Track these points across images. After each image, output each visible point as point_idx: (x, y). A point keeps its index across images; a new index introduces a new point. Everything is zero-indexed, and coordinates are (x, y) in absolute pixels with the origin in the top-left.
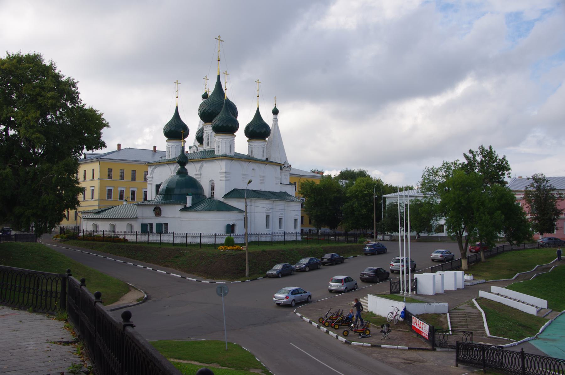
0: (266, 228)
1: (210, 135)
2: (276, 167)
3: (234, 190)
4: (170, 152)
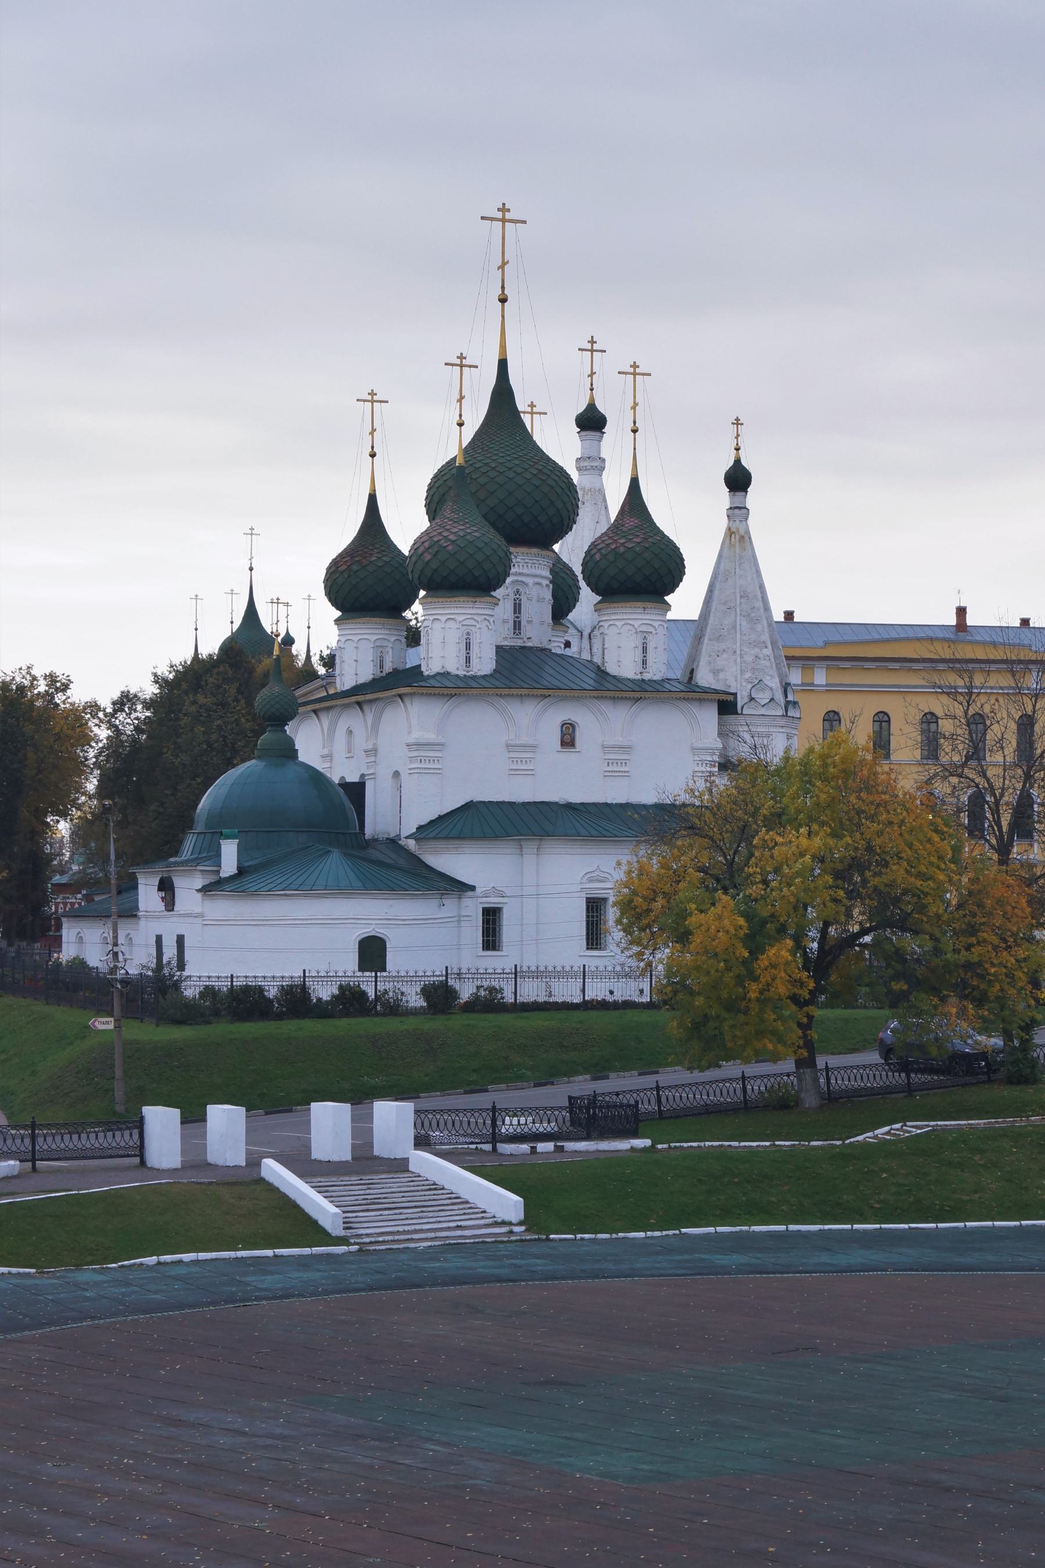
0: (588, 949)
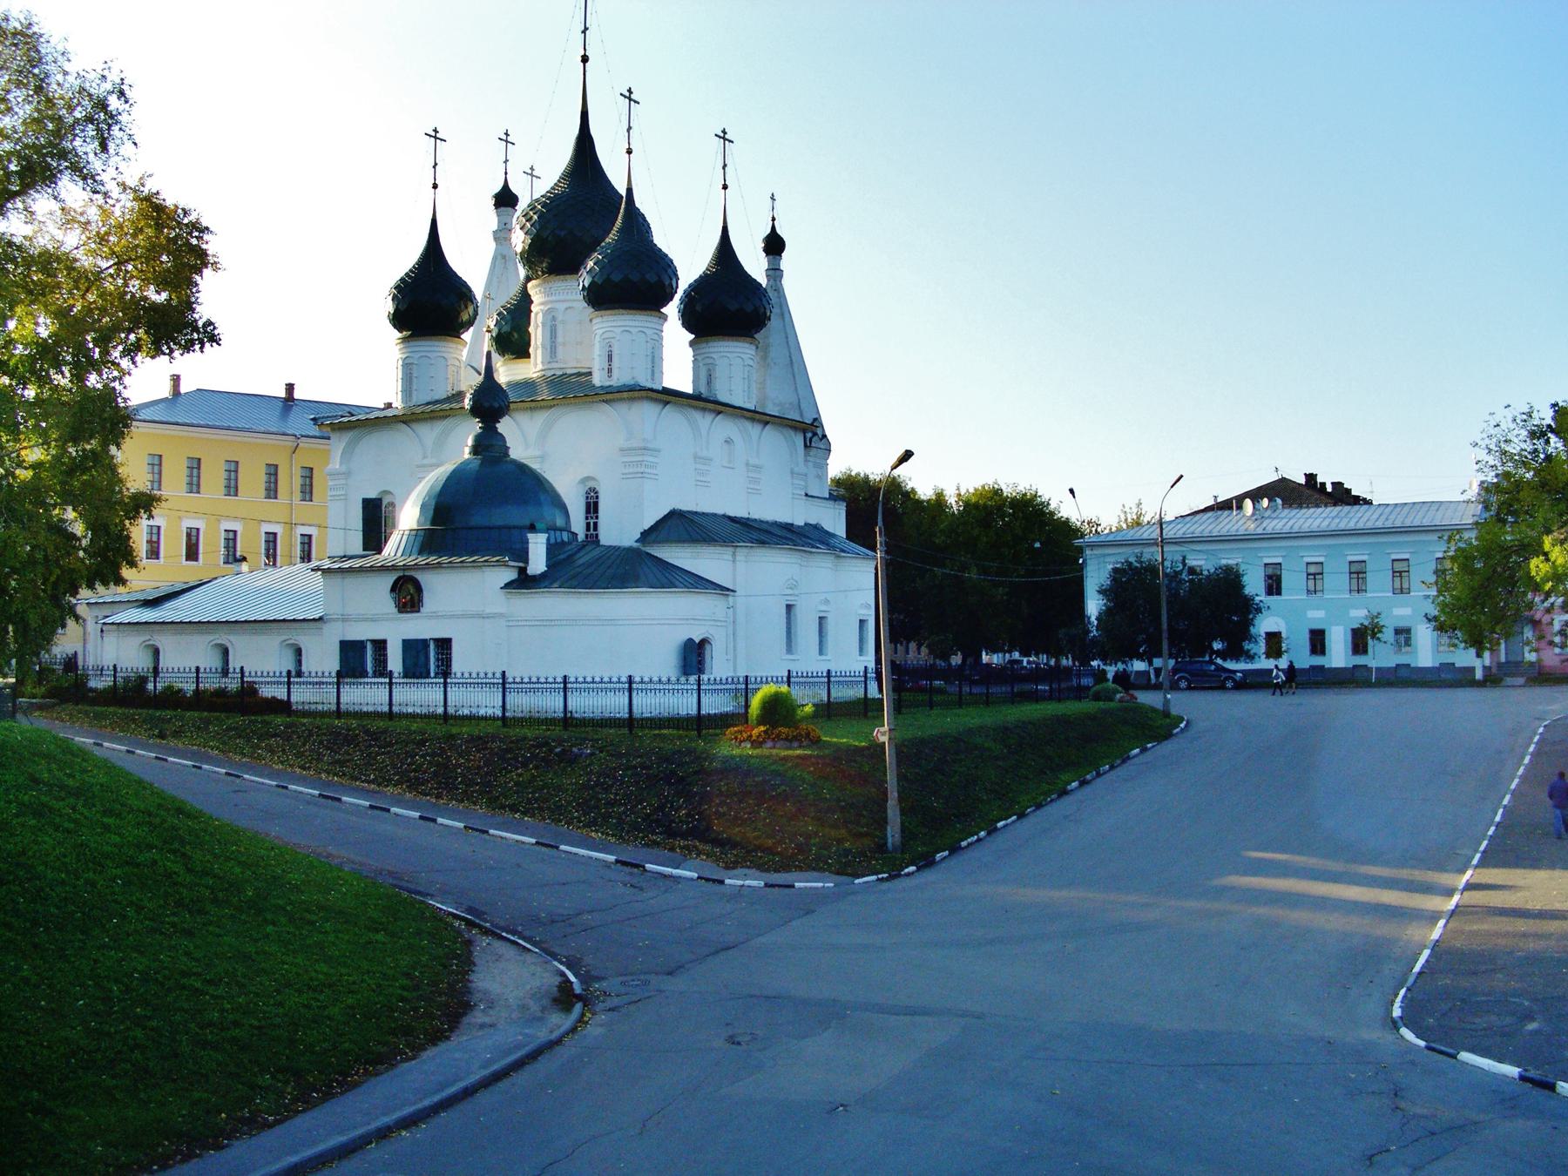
1: (560, 317)
2: (792, 433)
3: (674, 515)
4: (415, 380)
